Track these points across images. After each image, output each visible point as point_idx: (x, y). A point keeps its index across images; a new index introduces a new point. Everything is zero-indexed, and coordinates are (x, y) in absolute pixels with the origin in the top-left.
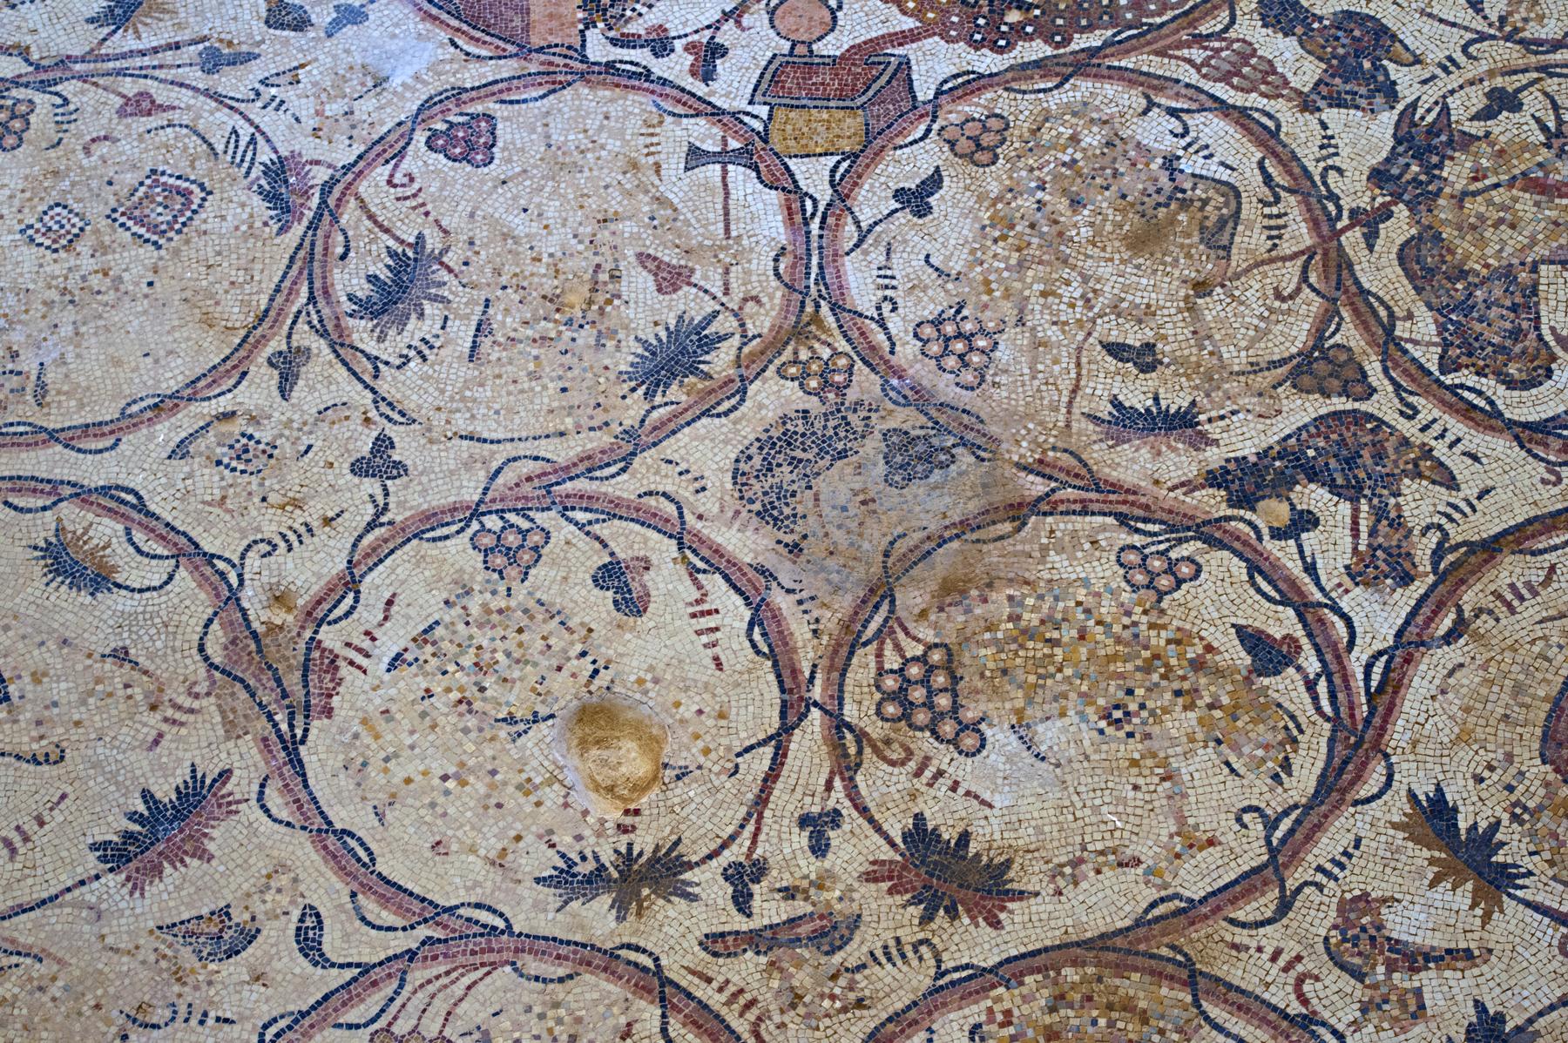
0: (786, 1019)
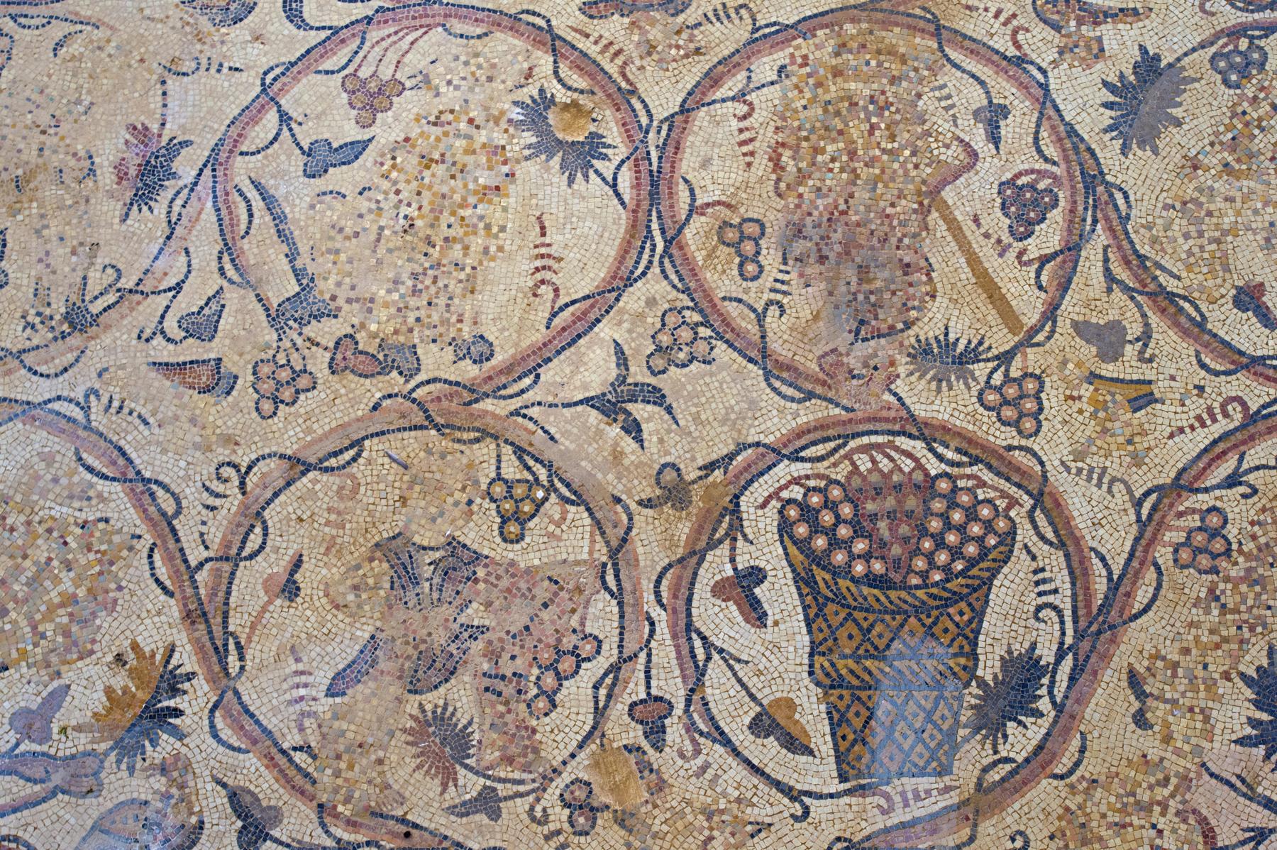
0: (645, 63)
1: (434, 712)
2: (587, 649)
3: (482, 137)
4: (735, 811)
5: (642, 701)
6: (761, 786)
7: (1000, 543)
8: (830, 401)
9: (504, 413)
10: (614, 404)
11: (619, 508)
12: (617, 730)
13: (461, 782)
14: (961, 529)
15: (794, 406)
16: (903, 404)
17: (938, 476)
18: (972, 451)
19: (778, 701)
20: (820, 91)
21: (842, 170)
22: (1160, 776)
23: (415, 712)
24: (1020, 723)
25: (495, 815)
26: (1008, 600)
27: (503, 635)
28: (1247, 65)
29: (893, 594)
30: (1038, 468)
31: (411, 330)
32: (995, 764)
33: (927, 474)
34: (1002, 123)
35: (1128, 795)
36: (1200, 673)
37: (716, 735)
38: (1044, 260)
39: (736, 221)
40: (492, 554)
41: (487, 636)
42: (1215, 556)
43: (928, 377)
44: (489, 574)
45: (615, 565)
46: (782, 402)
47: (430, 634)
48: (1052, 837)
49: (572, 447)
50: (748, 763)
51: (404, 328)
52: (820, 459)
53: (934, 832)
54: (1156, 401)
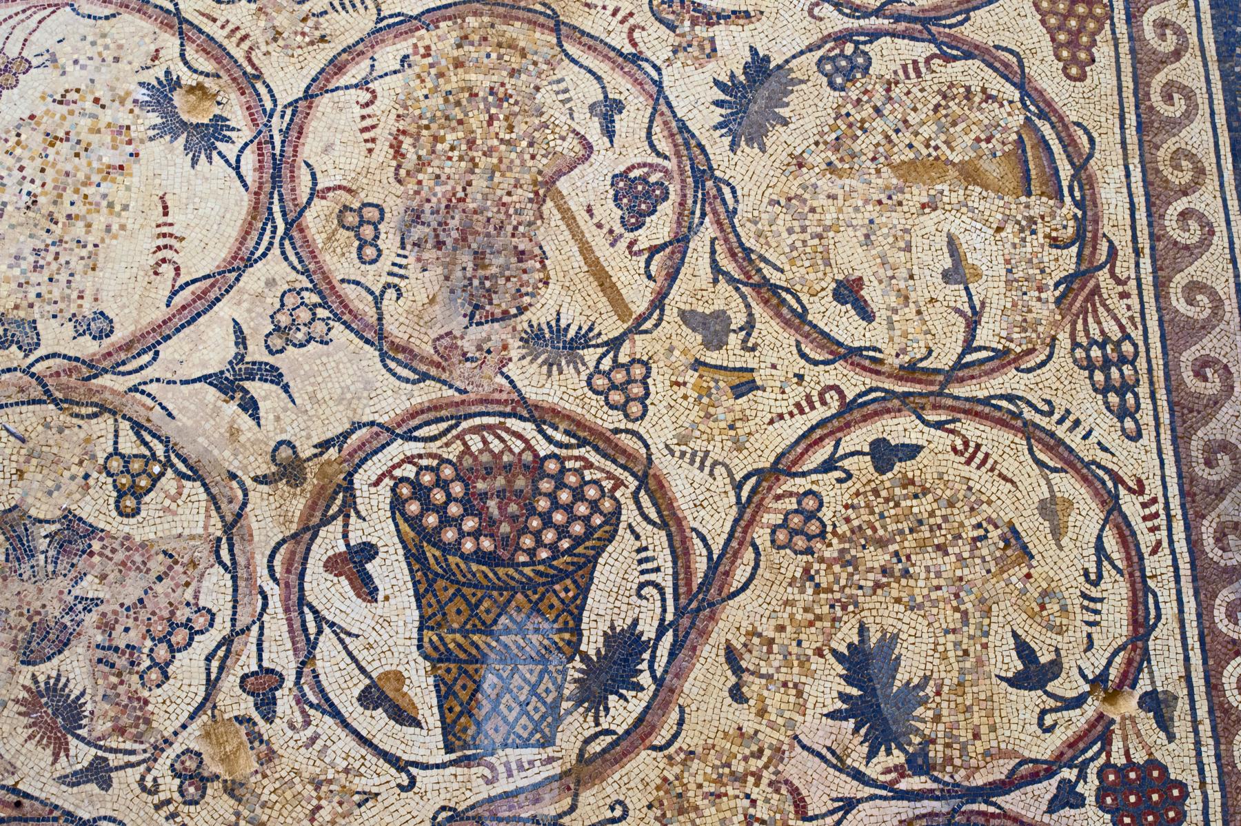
0: (270, 48)
1: (47, 683)
2: (200, 622)
3: (106, 117)
4: (343, 781)
5: (254, 674)
6: (369, 757)
7: (604, 523)
8: (444, 382)
9: (122, 389)
10: (232, 382)
11: (234, 484)
12: (228, 702)
13: (72, 752)
14: (568, 508)
15: (409, 386)
16: (515, 387)
17: (547, 457)
18: (581, 434)
19: (387, 673)
20: (441, 81)
21: (461, 159)
22: (755, 748)
23: (28, 683)
24: (622, 696)
25: (106, 784)
26: (612, 577)
27: (117, 607)
28: (852, 68)
29: (501, 571)
30: (643, 451)
31: (31, 306)
32: (595, 736)
33: (536, 455)
34: (617, 117)
35: (723, 766)
36: (794, 649)
37: (326, 707)
38: (654, 250)
39: (356, 205)
40: (108, 528)
41: (101, 608)
42: (810, 538)
43: (540, 361)
44: (104, 547)
45: (230, 540)
46: (397, 383)
47: (44, 606)
48: (650, 807)
49: (189, 423)
50: (356, 733)
51: (25, 304)
52: (433, 439)
53: (537, 801)
54: (758, 388)
